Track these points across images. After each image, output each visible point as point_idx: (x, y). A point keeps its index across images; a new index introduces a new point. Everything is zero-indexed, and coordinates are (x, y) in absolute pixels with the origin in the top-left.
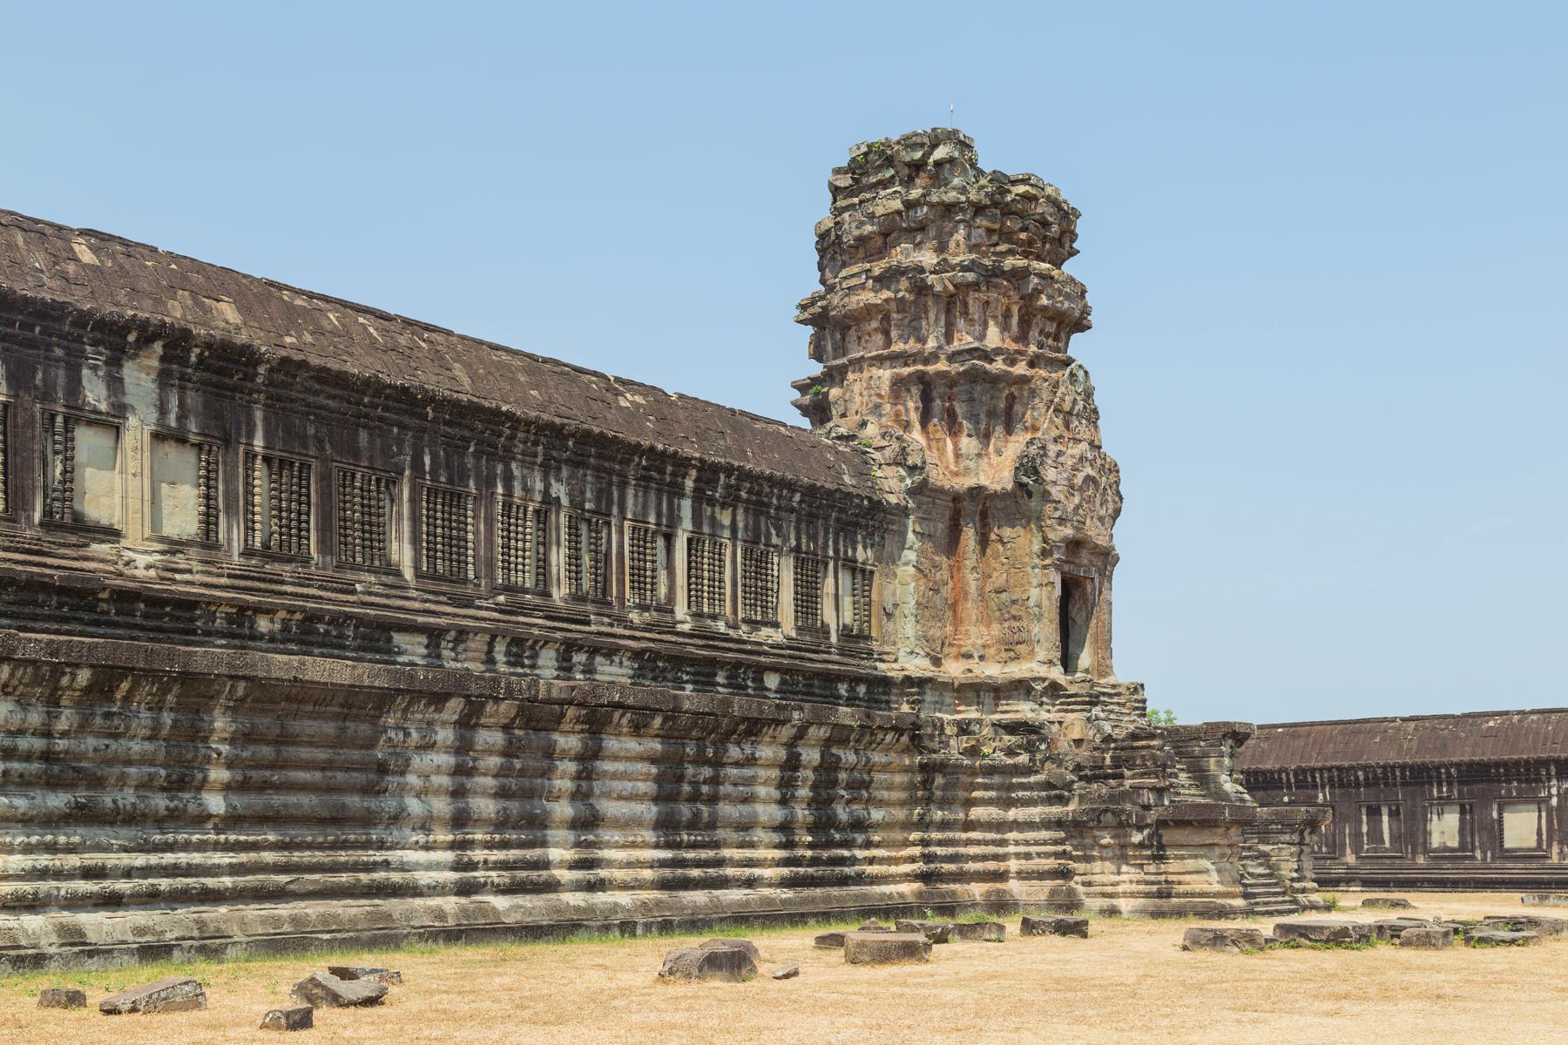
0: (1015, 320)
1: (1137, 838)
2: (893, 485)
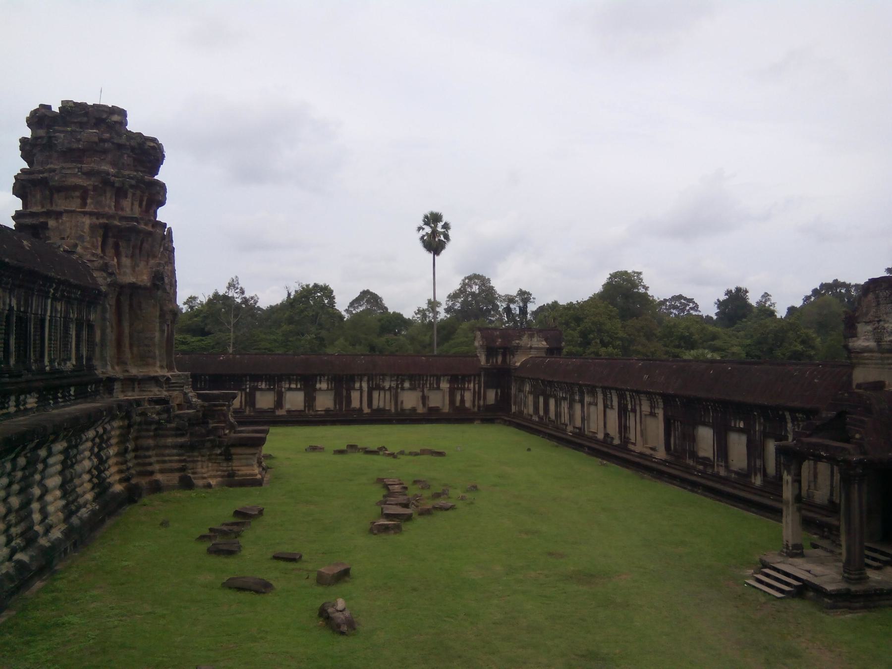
0: (144, 203)
2: (101, 280)
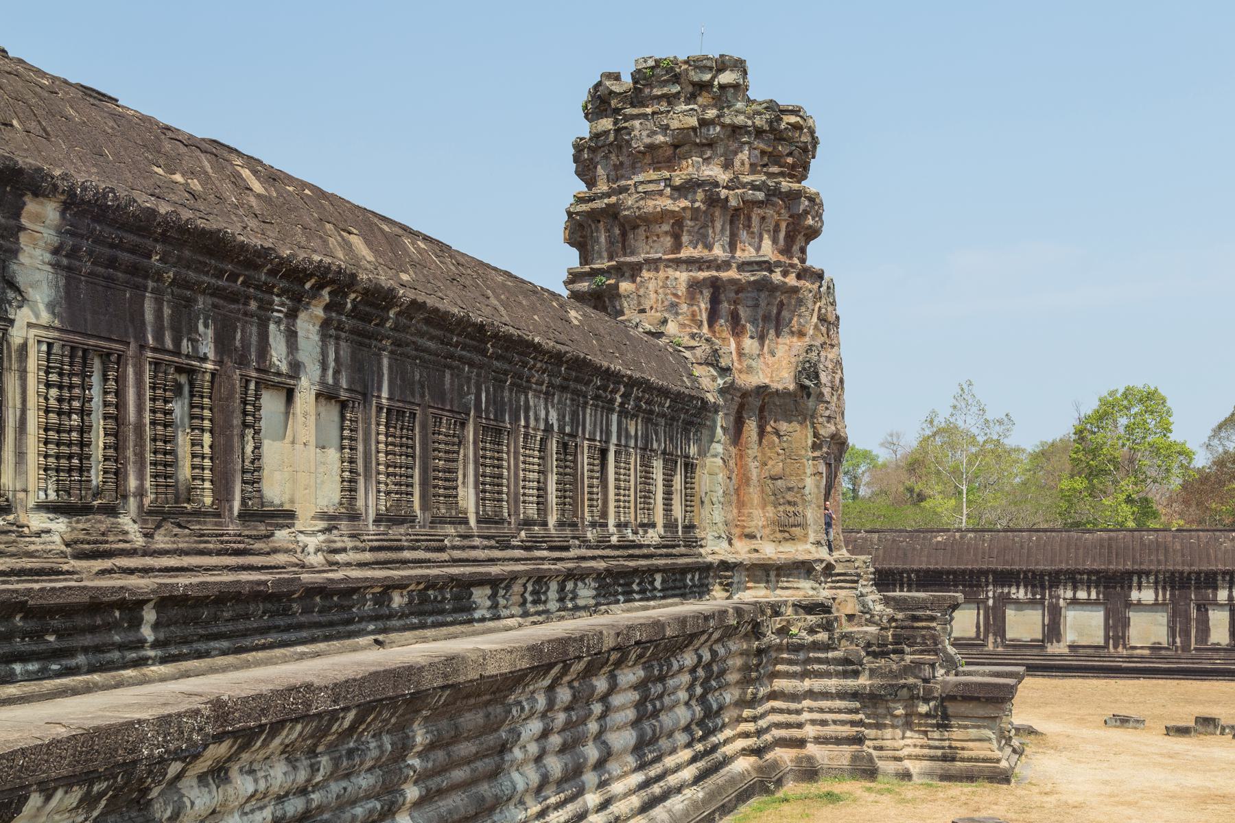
0: (782, 235)
1: (923, 708)
2: (709, 383)
